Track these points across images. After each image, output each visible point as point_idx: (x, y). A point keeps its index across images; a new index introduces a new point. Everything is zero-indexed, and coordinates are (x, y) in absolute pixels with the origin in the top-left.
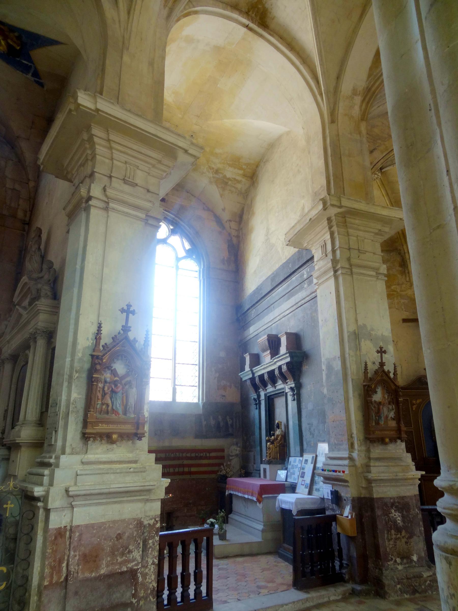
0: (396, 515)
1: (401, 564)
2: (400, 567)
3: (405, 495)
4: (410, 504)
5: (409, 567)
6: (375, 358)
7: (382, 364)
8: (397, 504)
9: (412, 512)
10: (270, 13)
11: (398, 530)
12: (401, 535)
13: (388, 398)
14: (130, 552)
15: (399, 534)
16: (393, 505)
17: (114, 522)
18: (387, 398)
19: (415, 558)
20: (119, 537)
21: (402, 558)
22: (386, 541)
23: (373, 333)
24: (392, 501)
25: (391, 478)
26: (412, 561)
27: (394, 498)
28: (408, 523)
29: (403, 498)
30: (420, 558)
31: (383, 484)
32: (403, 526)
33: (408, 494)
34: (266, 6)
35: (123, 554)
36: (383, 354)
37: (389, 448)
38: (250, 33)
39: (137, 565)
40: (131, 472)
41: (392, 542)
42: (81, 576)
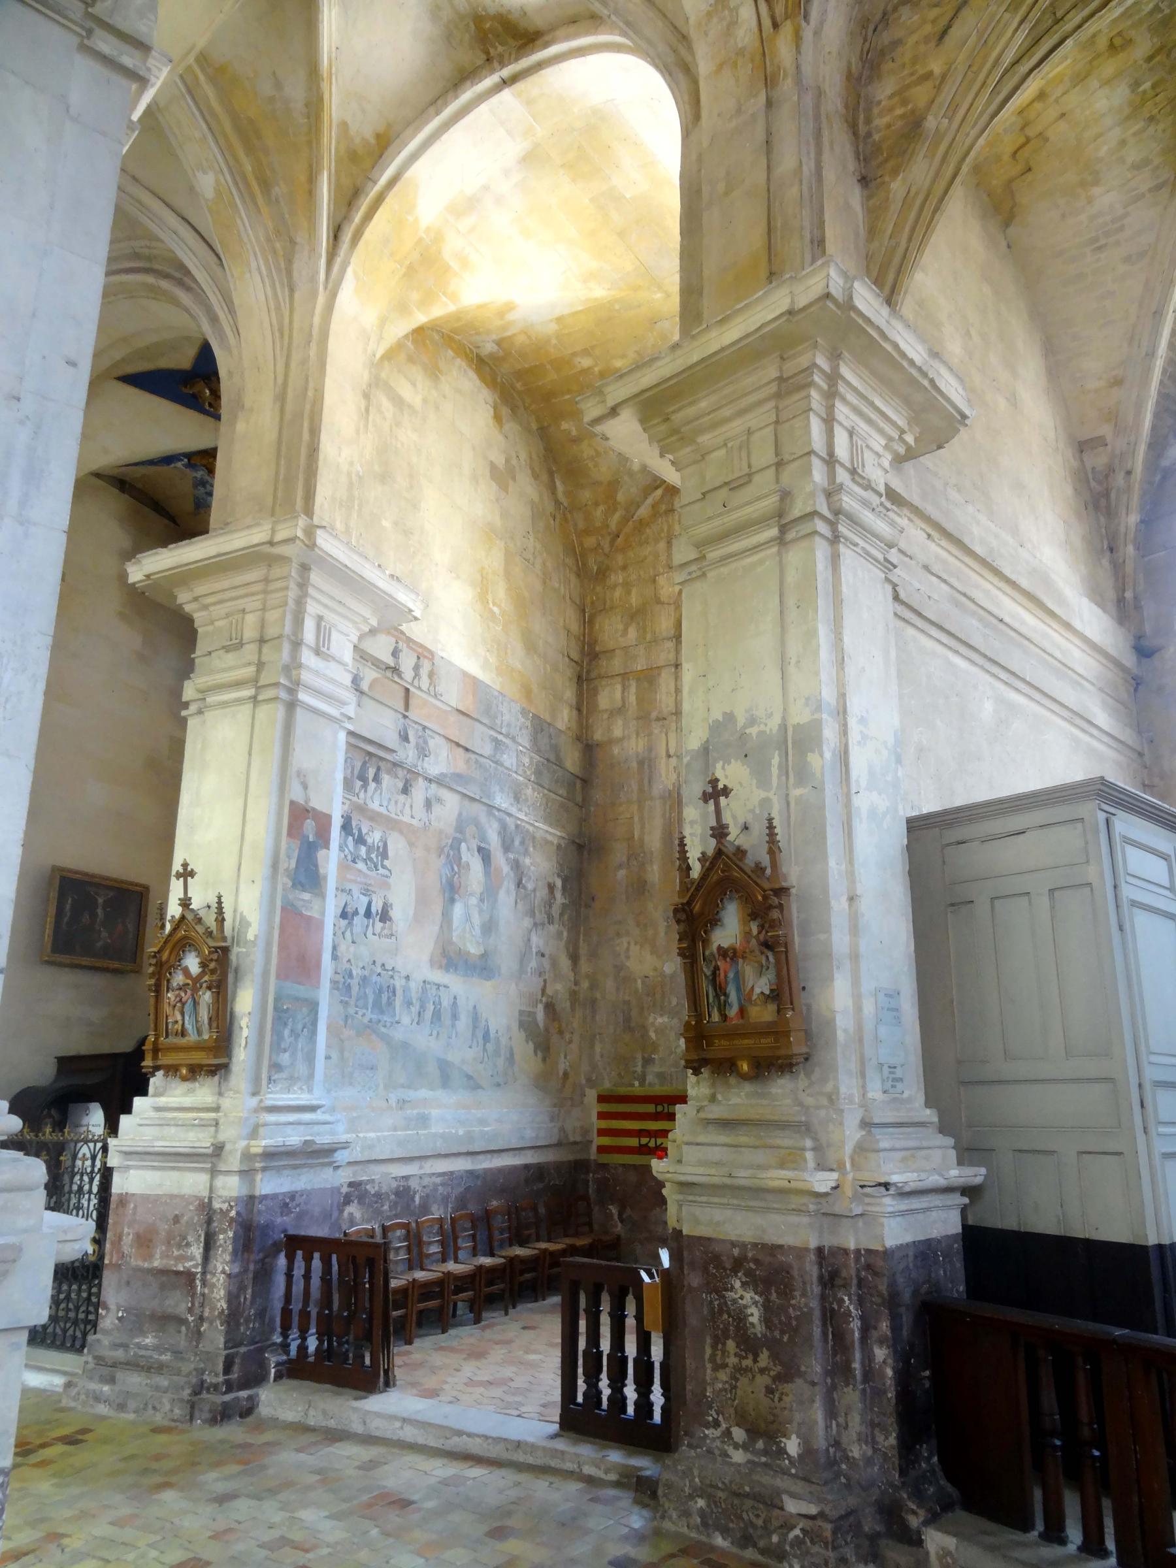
0: (748, 1301)
1: (745, 1447)
2: (738, 1457)
3: (781, 1242)
4: (795, 1273)
5: (765, 1465)
6: (752, 811)
7: (720, 832)
8: (752, 1266)
9: (798, 1299)
10: (509, 12)
11: (749, 1345)
12: (755, 1361)
13: (759, 933)
14: (188, 1245)
15: (751, 1357)
16: (738, 1264)
17: (172, 1196)
18: (755, 931)
19: (792, 1446)
20: (176, 1219)
21: (753, 1432)
22: (709, 1366)
23: (753, 731)
24: (736, 1252)
25: (716, 1180)
26: (782, 1452)
27: (743, 1246)
28: (783, 1332)
29: (774, 1249)
30: (808, 1452)
31: (704, 1199)
32: (765, 1336)
33: (788, 1240)
34: (492, 11)
35: (179, 1247)
36: (722, 799)
37: (774, 1090)
38: (520, 86)
39: (196, 1266)
40: (194, 1125)
41: (723, 1376)
42: (134, 1262)
